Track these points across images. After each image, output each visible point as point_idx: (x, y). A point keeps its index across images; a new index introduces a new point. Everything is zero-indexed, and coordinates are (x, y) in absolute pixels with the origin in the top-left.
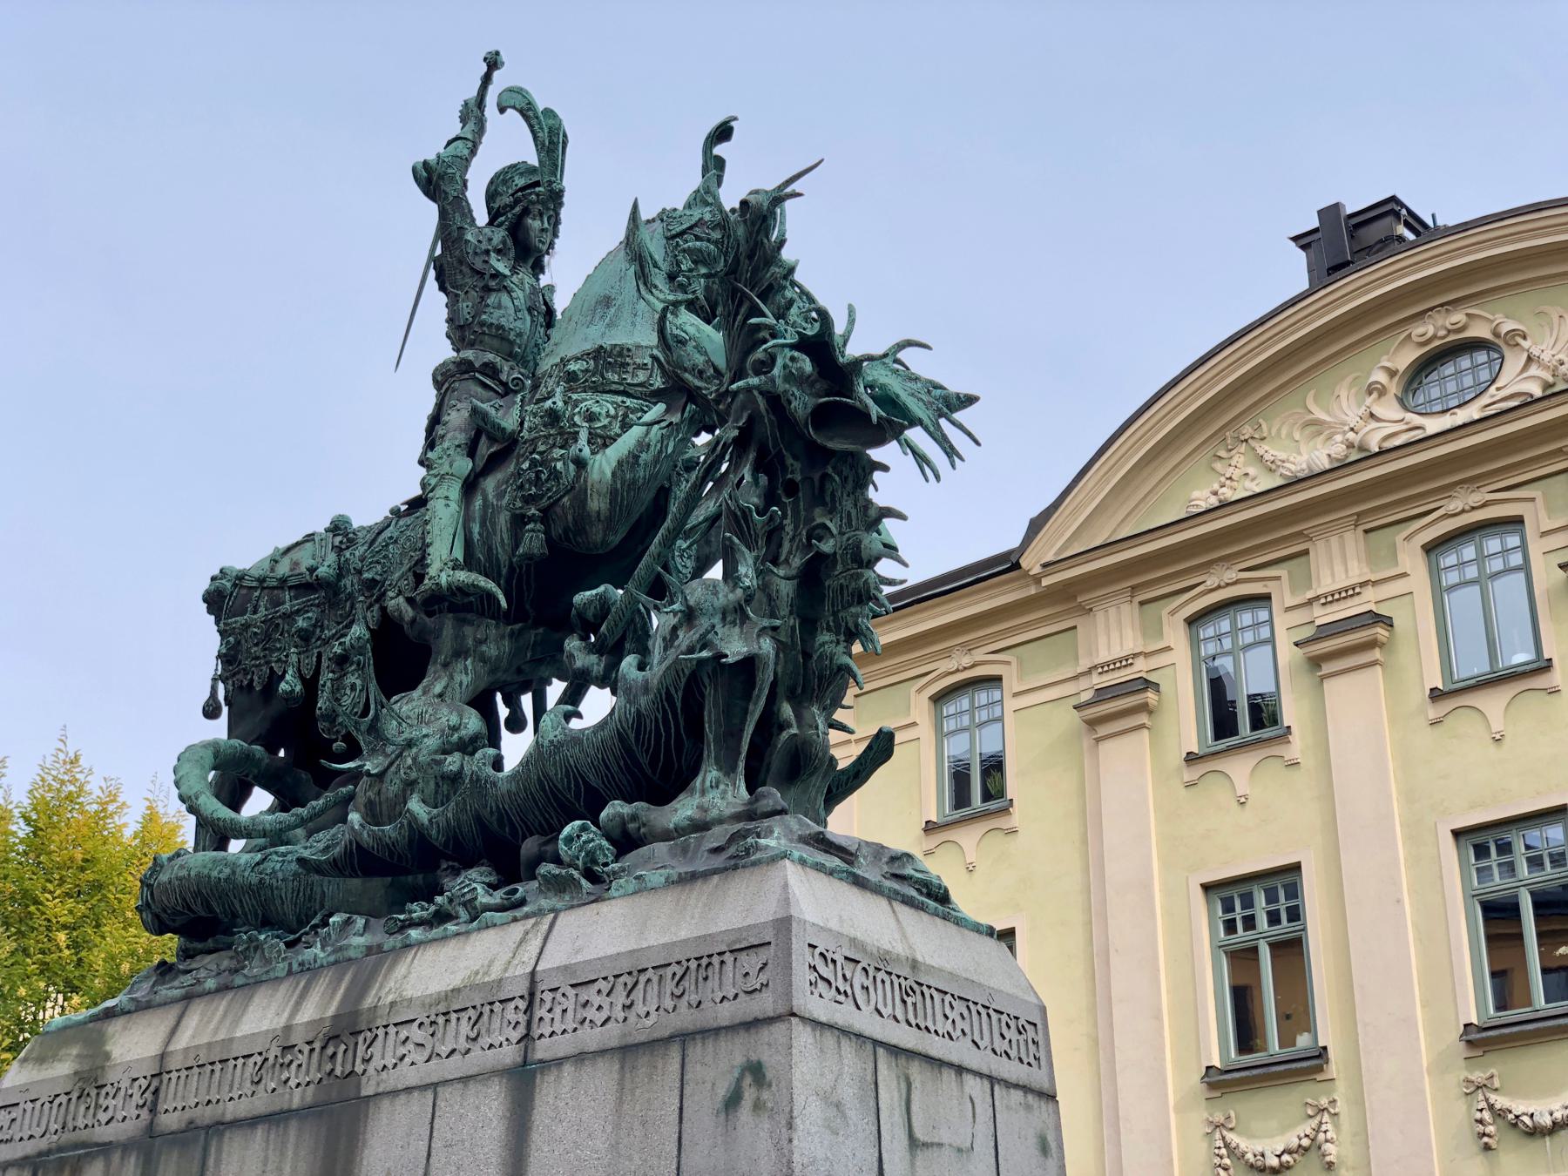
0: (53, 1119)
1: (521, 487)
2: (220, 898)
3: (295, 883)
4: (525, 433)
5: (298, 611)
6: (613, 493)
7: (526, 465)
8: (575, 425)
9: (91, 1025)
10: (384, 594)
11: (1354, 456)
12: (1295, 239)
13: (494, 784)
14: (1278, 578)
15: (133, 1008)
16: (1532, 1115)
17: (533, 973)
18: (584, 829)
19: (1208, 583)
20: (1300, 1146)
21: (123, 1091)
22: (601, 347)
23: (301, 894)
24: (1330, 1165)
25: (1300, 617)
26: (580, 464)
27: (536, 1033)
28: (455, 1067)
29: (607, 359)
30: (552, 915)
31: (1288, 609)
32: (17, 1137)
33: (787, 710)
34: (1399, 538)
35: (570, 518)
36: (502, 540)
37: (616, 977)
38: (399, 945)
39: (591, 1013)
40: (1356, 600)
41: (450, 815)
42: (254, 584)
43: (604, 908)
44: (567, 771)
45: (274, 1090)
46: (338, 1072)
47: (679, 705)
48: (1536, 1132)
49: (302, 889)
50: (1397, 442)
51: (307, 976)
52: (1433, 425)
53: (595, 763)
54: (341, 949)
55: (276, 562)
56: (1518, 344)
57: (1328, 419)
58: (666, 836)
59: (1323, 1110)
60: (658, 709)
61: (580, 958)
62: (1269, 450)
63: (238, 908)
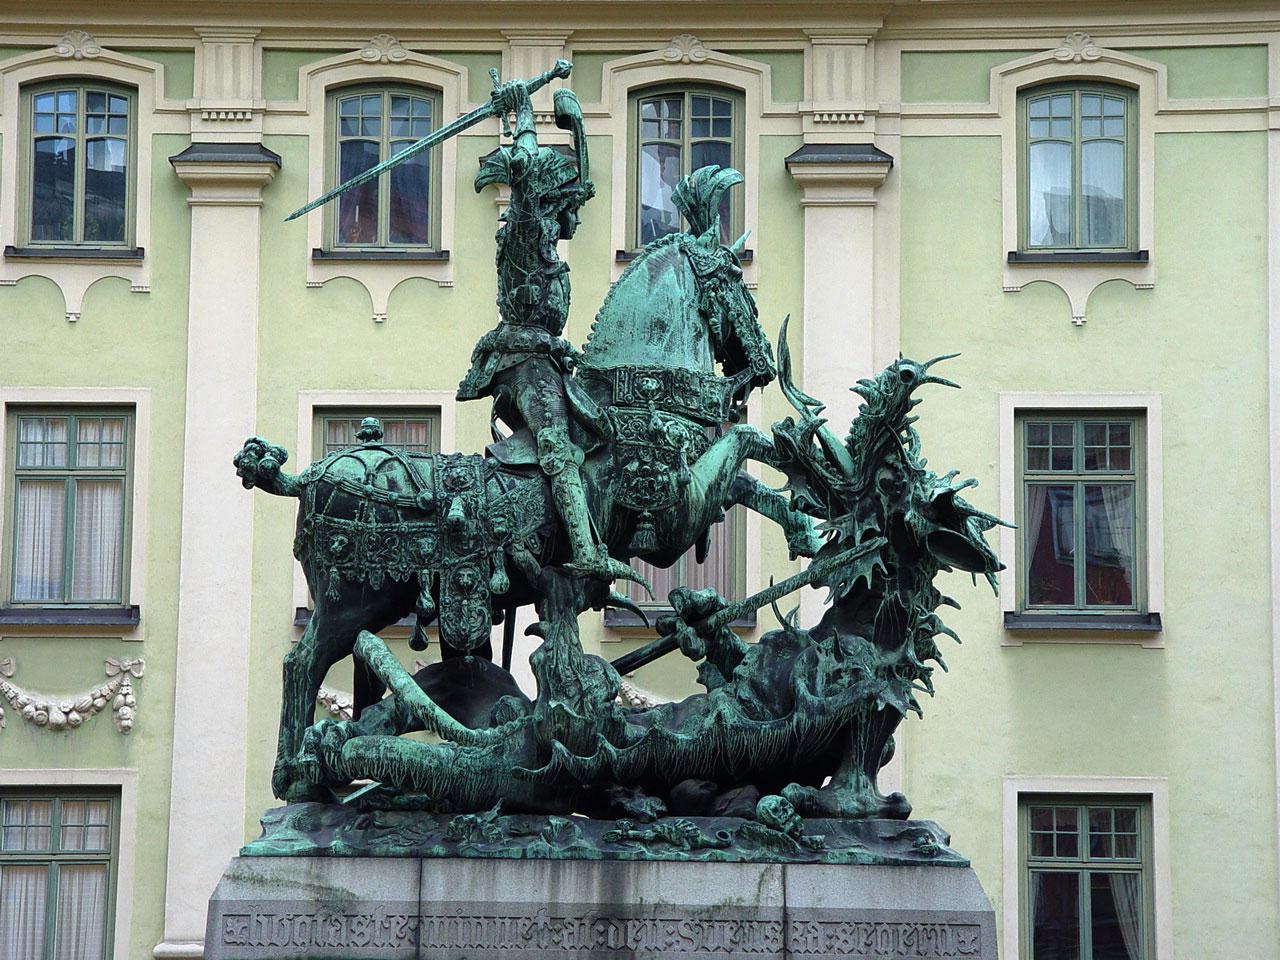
0: (296, 934)
4: (620, 436)
7: (634, 466)
8: (668, 444)
10: (513, 542)
13: (674, 742)
15: (349, 853)
17: (785, 908)
18: (782, 803)
19: (61, 49)
20: (93, 705)
21: (378, 924)
24: (127, 729)
25: (176, 125)
26: (683, 484)
27: (793, 947)
31: (158, 112)
32: (255, 942)
34: (304, 70)
35: (675, 525)
36: (603, 519)
38: (634, 857)
39: (838, 944)
40: (244, 126)
41: (632, 756)
42: (360, 494)
43: (829, 870)
45: (546, 947)
51: (548, 866)
54: (575, 848)
59: (125, 672)
61: (823, 905)
63: (434, 789)
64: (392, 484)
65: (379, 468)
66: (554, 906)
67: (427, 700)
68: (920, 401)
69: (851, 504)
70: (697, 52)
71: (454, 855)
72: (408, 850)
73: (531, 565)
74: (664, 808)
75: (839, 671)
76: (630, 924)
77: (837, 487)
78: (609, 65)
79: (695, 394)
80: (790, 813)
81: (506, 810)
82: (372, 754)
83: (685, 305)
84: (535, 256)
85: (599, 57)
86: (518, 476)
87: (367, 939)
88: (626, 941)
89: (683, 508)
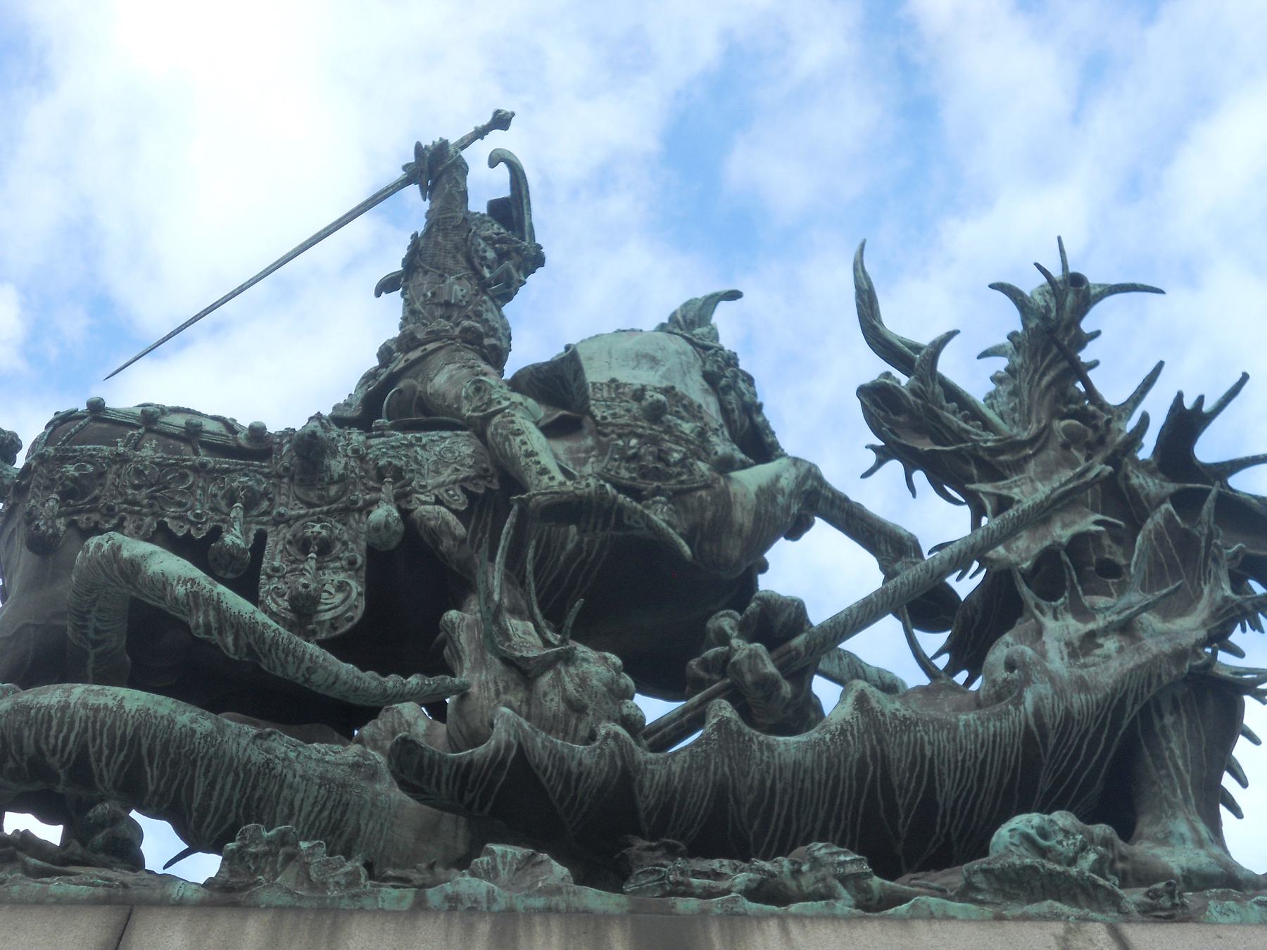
2: (175, 764)
3: (323, 791)
5: (227, 471)
6: (758, 517)
10: (411, 493)
22: (673, 388)
23: (326, 813)
35: (709, 515)
41: (676, 768)
44: (913, 763)
47: (1125, 723)
49: (329, 805)
53: (968, 763)
54: (558, 890)
60: (1098, 717)
63: (197, 800)
67: (198, 574)
68: (1097, 334)
69: (1018, 466)
72: (101, 891)
73: (447, 524)
75: (1091, 635)
77: (989, 444)
84: (460, 257)
89: (725, 502)
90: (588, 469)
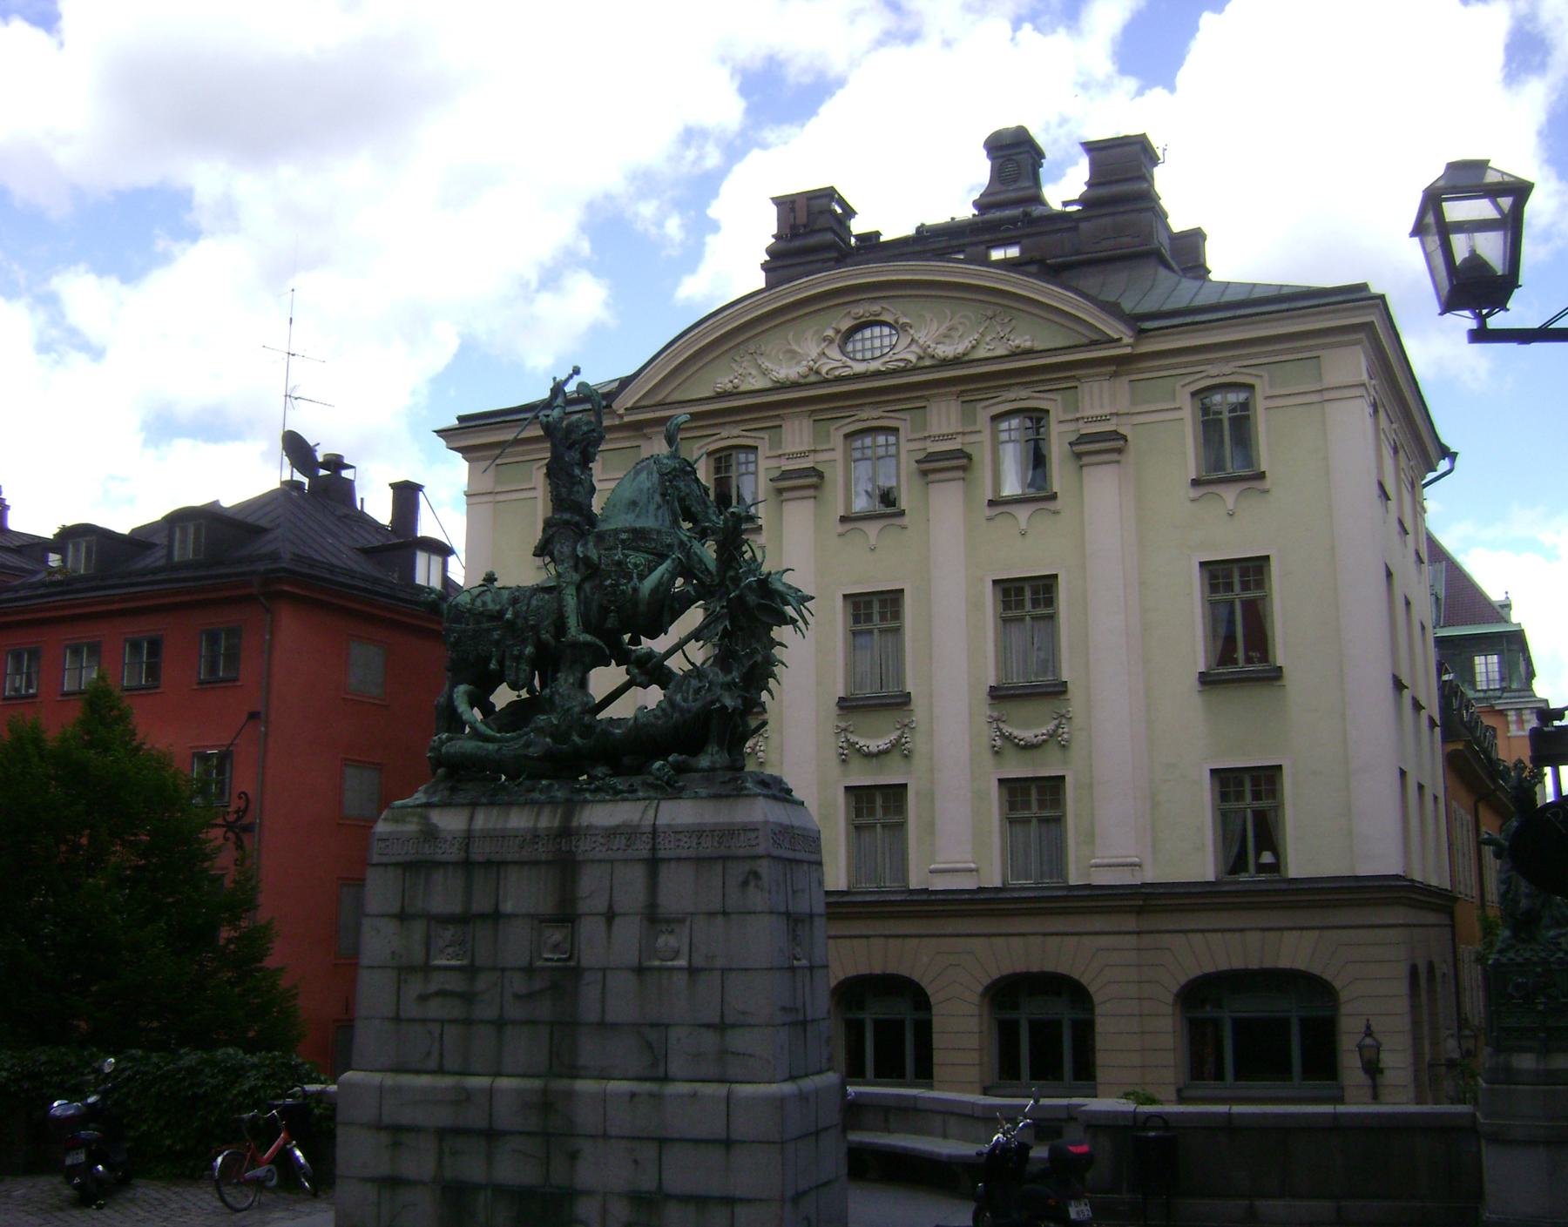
1: (606, 594)
4: (603, 566)
9: (419, 810)
11: (813, 378)
12: (773, 199)
13: (613, 734)
14: (763, 438)
16: (868, 747)
17: (654, 824)
18: (664, 765)
19: (722, 434)
24: (762, 762)
25: (773, 463)
26: (635, 590)
28: (619, 855)
29: (638, 537)
30: (656, 801)
33: (739, 721)
34: (832, 428)
37: (694, 832)
39: (682, 844)
40: (806, 459)
46: (563, 849)
48: (869, 755)
50: (837, 373)
52: (859, 368)
54: (552, 797)
55: (474, 600)
56: (906, 331)
57: (800, 351)
58: (697, 770)
61: (673, 822)
62: (767, 364)
64: (484, 604)
65: (479, 595)
66: (535, 829)
70: (1024, 393)
71: (492, 804)
74: (610, 772)
75: (700, 688)
76: (573, 838)
78: (980, 405)
79: (654, 539)
80: (666, 770)
81: (529, 777)
82: (452, 750)
83: (651, 491)
85: (974, 403)
86: (548, 593)
87: (443, 850)
88: (571, 847)
90: (596, 596)
